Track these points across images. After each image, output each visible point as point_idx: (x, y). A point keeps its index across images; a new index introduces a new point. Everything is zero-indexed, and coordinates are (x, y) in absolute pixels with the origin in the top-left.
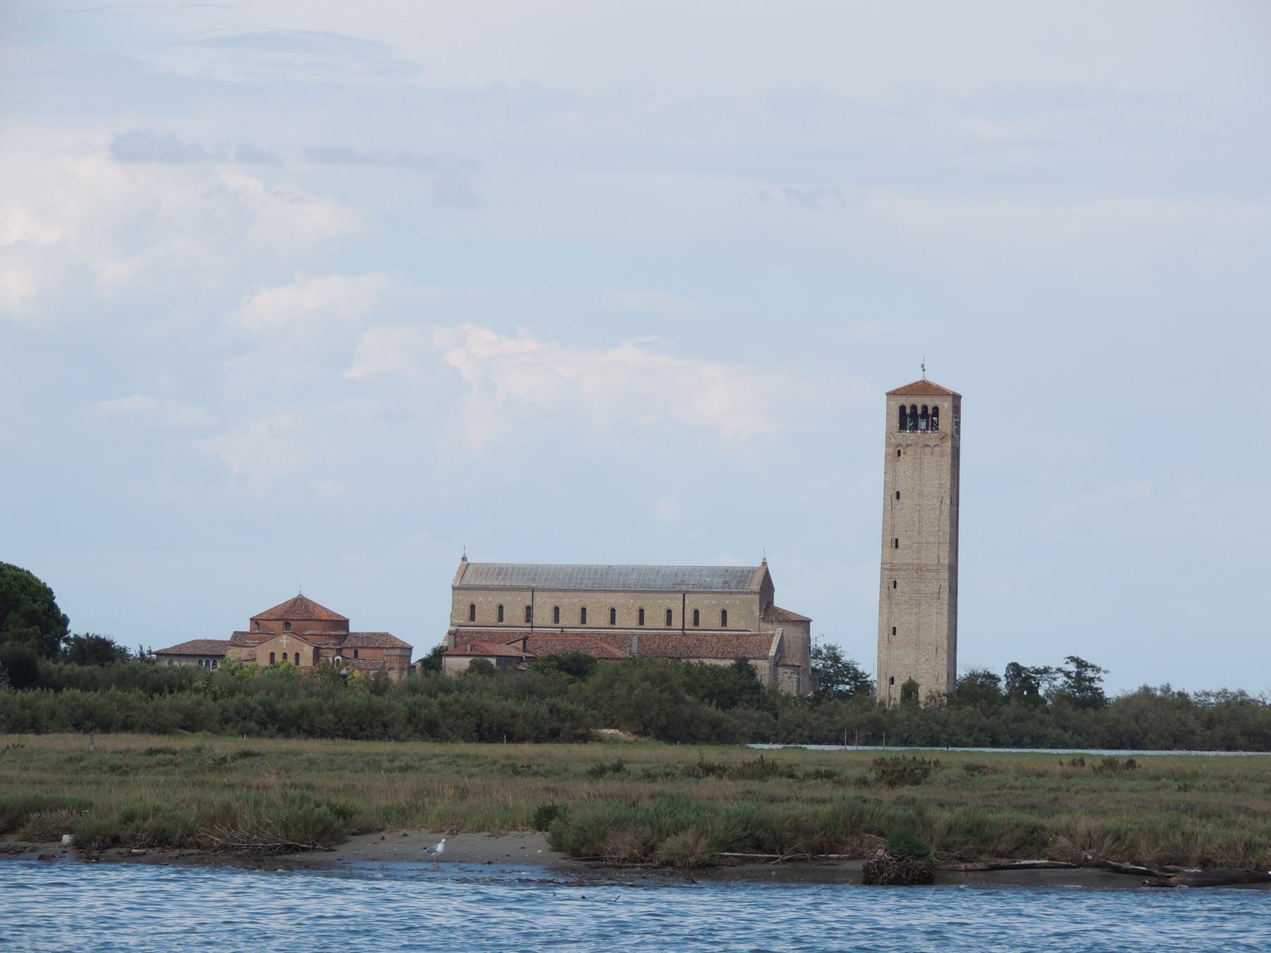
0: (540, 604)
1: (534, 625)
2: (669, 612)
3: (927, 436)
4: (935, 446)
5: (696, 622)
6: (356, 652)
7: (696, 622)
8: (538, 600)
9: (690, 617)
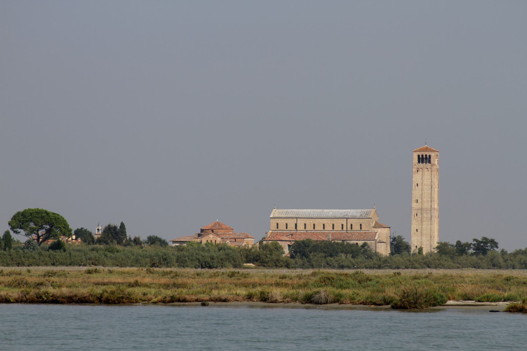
1: (297, 230)
2: (342, 225)
5: (351, 228)
6: (235, 240)
7: (351, 228)
9: (349, 227)
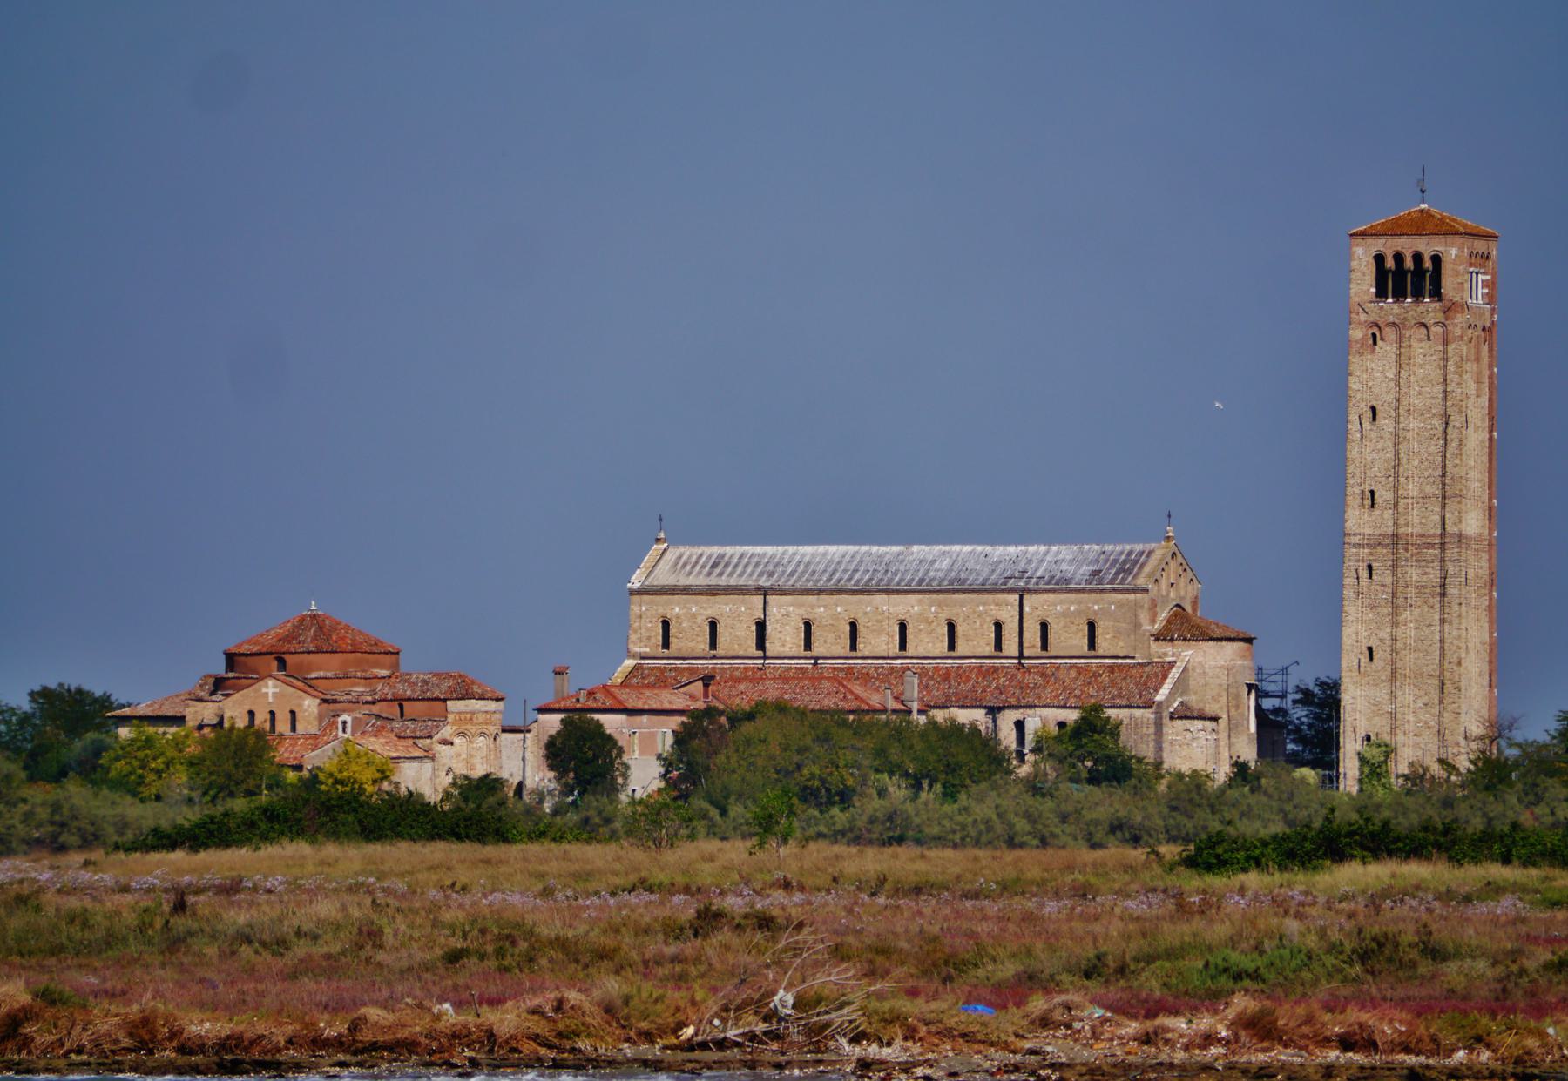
0: (779, 616)
1: (769, 654)
2: (998, 626)
3: (1421, 308)
8: (775, 610)
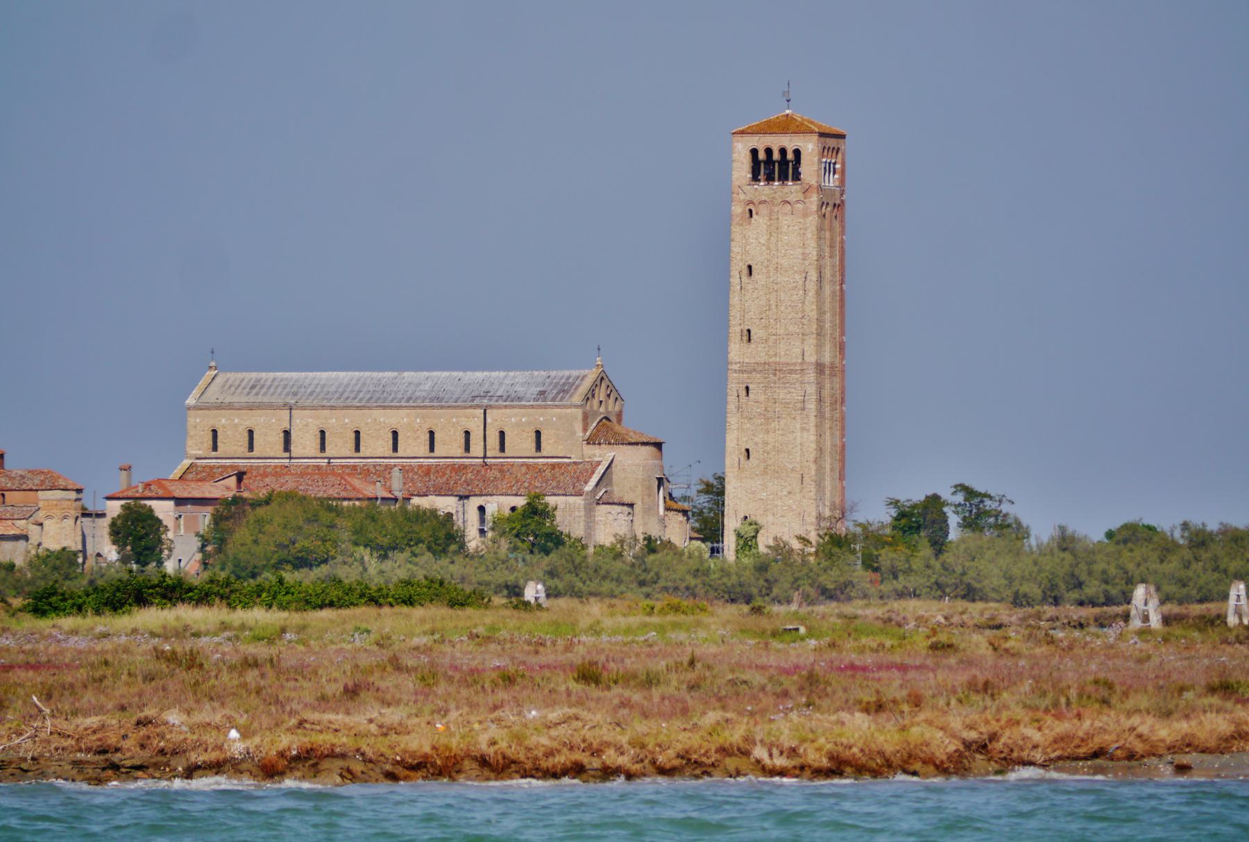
2: (467, 433)
3: (786, 190)
4: (798, 202)
9: (493, 440)
